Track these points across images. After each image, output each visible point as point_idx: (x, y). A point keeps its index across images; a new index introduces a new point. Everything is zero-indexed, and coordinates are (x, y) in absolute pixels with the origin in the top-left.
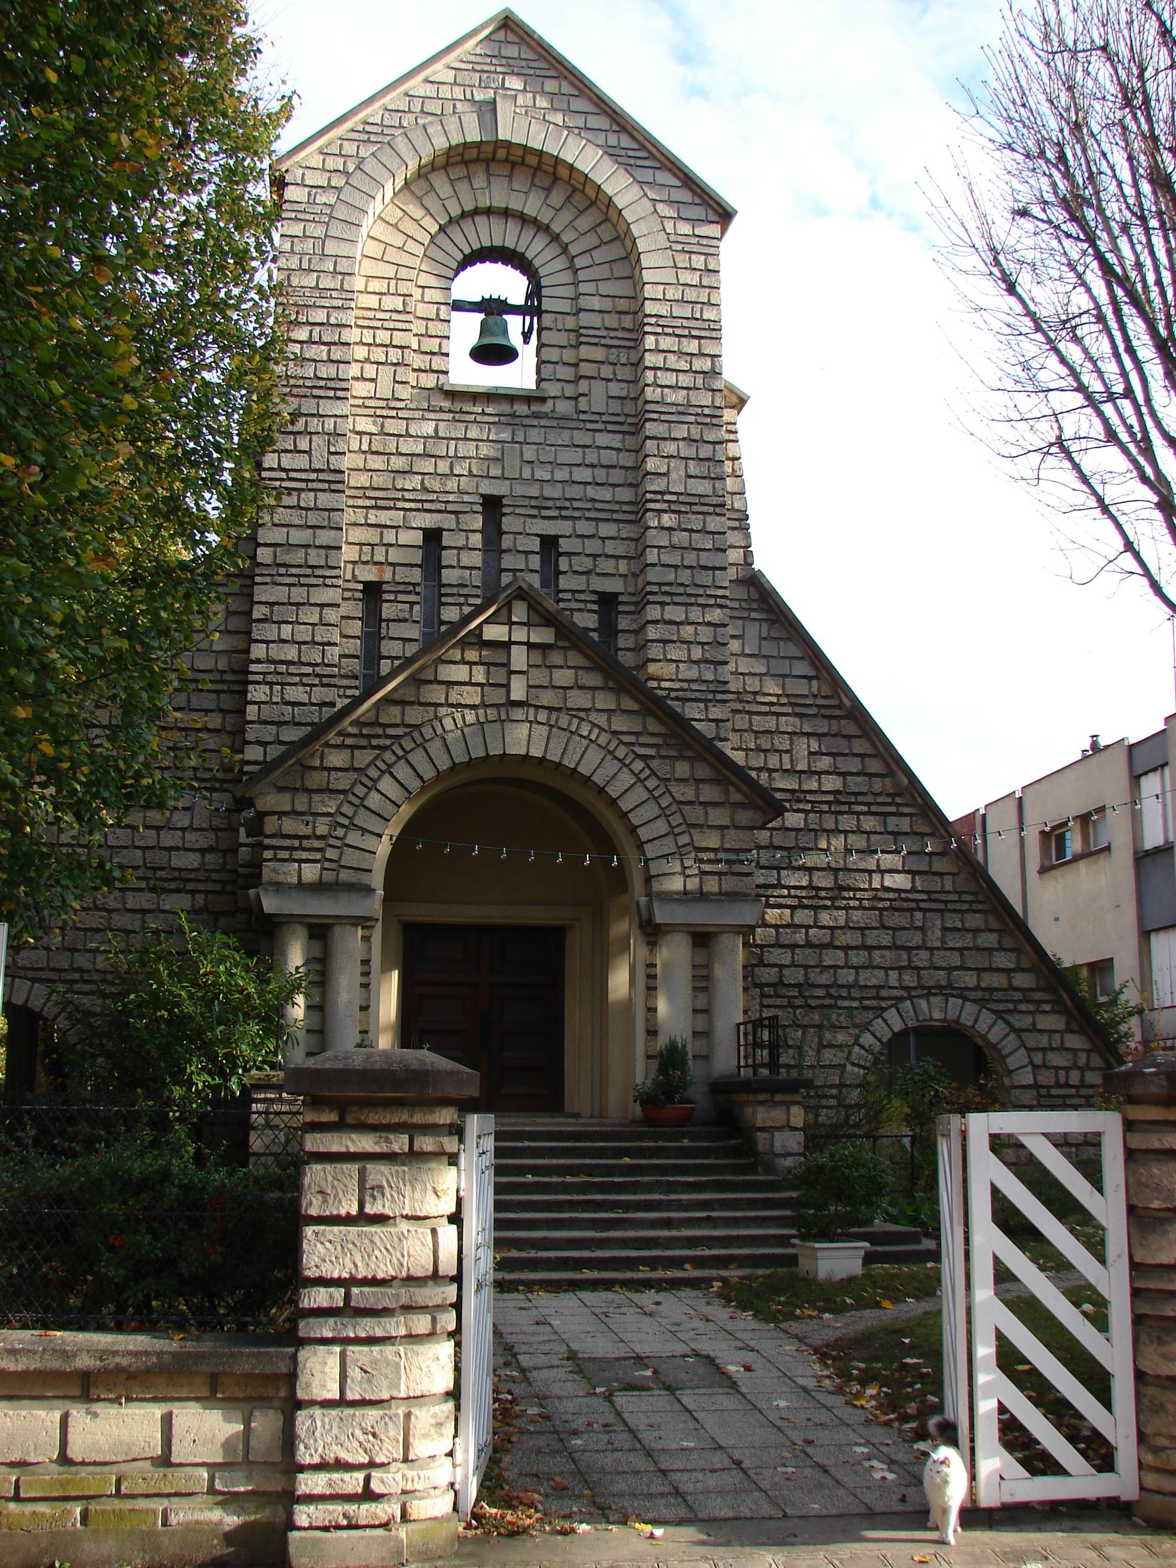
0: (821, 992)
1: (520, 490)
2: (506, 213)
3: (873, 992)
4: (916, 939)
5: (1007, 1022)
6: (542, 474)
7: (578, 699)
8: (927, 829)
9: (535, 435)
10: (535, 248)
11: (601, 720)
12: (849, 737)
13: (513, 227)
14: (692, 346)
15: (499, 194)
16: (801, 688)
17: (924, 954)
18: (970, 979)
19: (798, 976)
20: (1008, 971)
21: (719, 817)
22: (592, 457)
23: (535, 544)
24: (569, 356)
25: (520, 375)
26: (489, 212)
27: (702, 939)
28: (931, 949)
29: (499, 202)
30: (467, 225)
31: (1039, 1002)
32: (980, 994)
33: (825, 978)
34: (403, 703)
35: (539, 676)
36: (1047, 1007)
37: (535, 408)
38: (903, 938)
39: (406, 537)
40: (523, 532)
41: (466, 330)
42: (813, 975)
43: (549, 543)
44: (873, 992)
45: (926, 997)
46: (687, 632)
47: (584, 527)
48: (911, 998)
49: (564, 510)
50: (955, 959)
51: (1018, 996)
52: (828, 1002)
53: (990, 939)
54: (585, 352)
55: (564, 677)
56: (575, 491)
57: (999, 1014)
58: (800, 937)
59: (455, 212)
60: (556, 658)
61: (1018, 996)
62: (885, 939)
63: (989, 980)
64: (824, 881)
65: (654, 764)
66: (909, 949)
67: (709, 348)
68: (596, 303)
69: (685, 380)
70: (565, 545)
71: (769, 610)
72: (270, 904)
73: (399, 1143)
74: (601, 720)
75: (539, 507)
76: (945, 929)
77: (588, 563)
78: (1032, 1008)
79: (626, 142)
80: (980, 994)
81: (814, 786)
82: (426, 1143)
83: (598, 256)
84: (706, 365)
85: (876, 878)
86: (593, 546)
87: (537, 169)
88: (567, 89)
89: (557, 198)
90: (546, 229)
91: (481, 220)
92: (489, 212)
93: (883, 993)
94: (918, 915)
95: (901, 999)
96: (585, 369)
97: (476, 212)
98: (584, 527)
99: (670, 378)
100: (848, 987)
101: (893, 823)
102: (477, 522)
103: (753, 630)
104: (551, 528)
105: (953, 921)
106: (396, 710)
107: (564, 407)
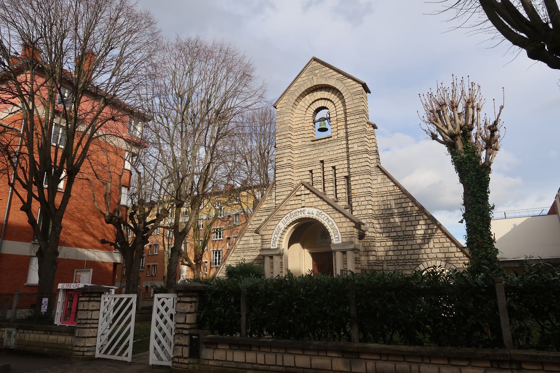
0: (402, 261)
1: (327, 158)
2: (322, 99)
3: (415, 261)
9: (329, 145)
11: (320, 207)
17: (429, 250)
19: (396, 258)
23: (331, 169)
26: (318, 100)
27: (344, 253)
33: (402, 258)
37: (330, 139)
39: (306, 173)
42: (400, 258)
44: (415, 261)
46: (360, 182)
47: (340, 163)
49: (336, 160)
52: (404, 263)
54: (339, 124)
55: (312, 200)
56: (338, 155)
59: (311, 102)
60: (311, 196)
64: (400, 234)
69: (356, 125)
70: (336, 168)
73: (88, 299)
74: (320, 207)
75: (331, 160)
79: (341, 75)
82: (92, 299)
88: (327, 68)
96: (339, 128)
97: (315, 101)
98: (340, 163)
99: (353, 125)
104: (333, 165)
107: (336, 137)
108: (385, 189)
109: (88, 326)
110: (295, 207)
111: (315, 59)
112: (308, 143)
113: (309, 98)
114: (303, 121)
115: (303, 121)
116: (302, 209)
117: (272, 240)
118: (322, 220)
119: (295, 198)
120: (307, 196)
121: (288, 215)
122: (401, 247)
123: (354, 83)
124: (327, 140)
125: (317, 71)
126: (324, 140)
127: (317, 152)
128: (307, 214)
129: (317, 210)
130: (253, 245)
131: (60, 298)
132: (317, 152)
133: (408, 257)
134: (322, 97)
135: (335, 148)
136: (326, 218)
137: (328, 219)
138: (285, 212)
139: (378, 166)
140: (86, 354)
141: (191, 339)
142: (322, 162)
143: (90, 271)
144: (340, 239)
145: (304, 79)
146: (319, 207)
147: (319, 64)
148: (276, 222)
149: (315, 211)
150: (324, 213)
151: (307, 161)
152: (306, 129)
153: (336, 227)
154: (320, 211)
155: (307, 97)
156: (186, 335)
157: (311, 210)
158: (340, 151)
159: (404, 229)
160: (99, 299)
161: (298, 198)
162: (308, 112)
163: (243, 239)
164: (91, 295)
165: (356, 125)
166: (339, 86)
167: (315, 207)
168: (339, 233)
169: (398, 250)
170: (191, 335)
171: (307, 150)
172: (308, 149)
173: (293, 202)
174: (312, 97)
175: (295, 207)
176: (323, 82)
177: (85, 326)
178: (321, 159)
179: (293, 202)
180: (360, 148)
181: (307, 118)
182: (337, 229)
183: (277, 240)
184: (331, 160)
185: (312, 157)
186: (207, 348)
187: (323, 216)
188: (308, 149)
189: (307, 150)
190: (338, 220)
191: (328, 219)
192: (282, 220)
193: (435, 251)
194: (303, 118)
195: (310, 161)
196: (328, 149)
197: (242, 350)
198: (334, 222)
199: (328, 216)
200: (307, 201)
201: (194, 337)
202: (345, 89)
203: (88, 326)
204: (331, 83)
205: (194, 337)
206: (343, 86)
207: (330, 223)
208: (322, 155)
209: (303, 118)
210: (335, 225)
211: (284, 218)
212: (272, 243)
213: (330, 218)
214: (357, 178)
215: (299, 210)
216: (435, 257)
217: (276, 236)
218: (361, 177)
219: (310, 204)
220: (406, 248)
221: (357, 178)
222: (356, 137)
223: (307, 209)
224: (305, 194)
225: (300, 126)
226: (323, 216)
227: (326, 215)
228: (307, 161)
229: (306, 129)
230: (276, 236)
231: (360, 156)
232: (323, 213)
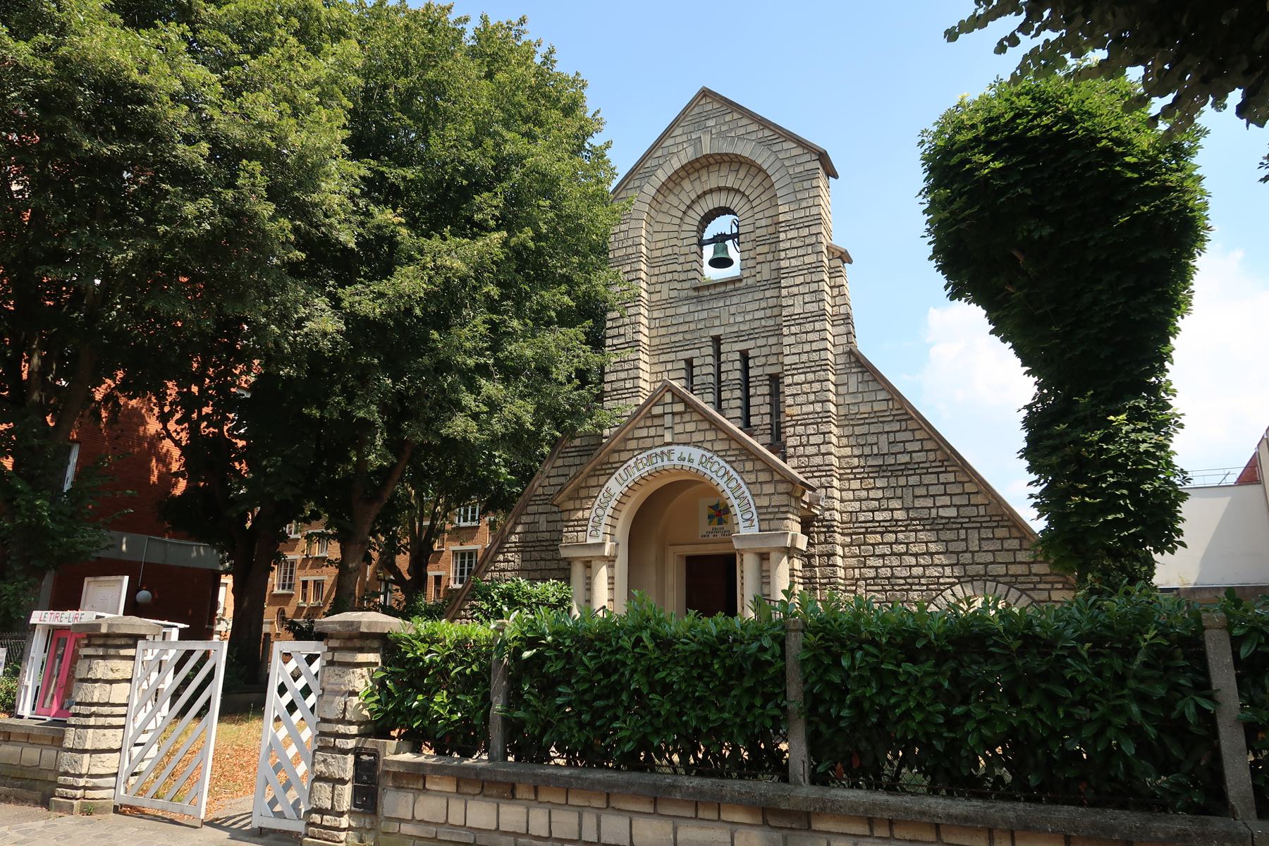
0: (902, 581)
1: (728, 330)
2: (720, 189)
4: (962, 546)
5: (1029, 596)
6: (740, 319)
7: (697, 437)
8: (967, 479)
9: (735, 300)
10: (735, 202)
11: (708, 446)
12: (913, 430)
13: (723, 195)
14: (805, 232)
15: (714, 180)
16: (883, 406)
18: (1001, 570)
19: (888, 572)
20: (1028, 563)
21: (768, 489)
22: (763, 304)
23: (737, 356)
24: (752, 254)
25: (733, 271)
28: (973, 553)
29: (714, 186)
30: (702, 202)
31: (1052, 583)
32: (1008, 579)
33: (905, 573)
34: (619, 451)
35: (678, 429)
36: (1060, 586)
37: (737, 285)
38: (952, 547)
39: (677, 365)
40: (731, 351)
41: (709, 252)
43: (745, 357)
45: (971, 582)
46: (806, 388)
47: (761, 342)
48: (960, 583)
49: (751, 335)
50: (990, 558)
51: (1036, 579)
53: (1014, 544)
56: (756, 324)
57: (1023, 591)
58: (887, 550)
59: (693, 196)
60: (687, 417)
61: (1036, 579)
62: (941, 547)
63: (1013, 569)
65: (735, 465)
66: (957, 553)
67: (814, 230)
68: (763, 223)
69: (801, 252)
70: (751, 353)
71: (862, 366)
72: (564, 553)
74: (708, 446)
75: (738, 336)
76: (980, 539)
77: (763, 360)
78: (1048, 586)
79: (767, 132)
80: (1008, 579)
81: (893, 462)
82: (112, 652)
83: (764, 197)
84: (813, 240)
85: (934, 511)
86: (765, 351)
87: (731, 162)
88: (736, 116)
89: (742, 174)
90: (737, 191)
91: (708, 197)
92: (711, 191)
93: (941, 580)
94: (963, 532)
95: (953, 584)
97: (705, 193)
98: (761, 342)
99: (793, 253)
100: (919, 578)
101: (943, 478)
102: (710, 351)
103: (853, 380)
105: (987, 533)
106: (616, 455)
107: (750, 281)
108: (865, 408)
109: (101, 721)
110: (648, 442)
111: (705, 93)
112: (684, 294)
113: (690, 189)
114: (674, 242)
115: (674, 242)
116: (665, 449)
117: (591, 523)
118: (714, 476)
119: (649, 423)
120: (677, 419)
121: (631, 462)
122: (902, 548)
123: (799, 151)
124: (731, 287)
125: (711, 123)
126: (722, 289)
127: (704, 315)
128: (676, 462)
129: (701, 452)
130: (547, 536)
131: (37, 648)
132: (704, 315)
133: (917, 571)
134: (722, 184)
135: (750, 307)
136: (722, 472)
137: (727, 473)
138: (624, 456)
139: (851, 353)
140: (90, 794)
141: (357, 763)
142: (717, 340)
143: (121, 581)
144: (756, 522)
145: (679, 140)
146: (705, 445)
147: (716, 105)
148: (602, 479)
149: (696, 453)
150: (719, 460)
151: (680, 337)
152: (682, 259)
153: (747, 494)
154: (709, 455)
155: (687, 185)
156: (345, 752)
157: (686, 451)
158: (760, 314)
159: (909, 504)
160: (131, 652)
161: (657, 422)
162: (687, 220)
163: (524, 519)
164: (110, 642)
165: (801, 252)
166: (763, 158)
167: (697, 445)
168: (753, 509)
169: (893, 554)
170: (357, 752)
171: (680, 311)
172: (685, 309)
173: (644, 433)
174: (697, 182)
175: (648, 442)
176: (726, 148)
177: (92, 721)
178: (714, 332)
179: (644, 433)
180: (809, 307)
181: (683, 235)
182: (750, 497)
183: (603, 522)
184: (738, 336)
185: (693, 326)
186: (399, 788)
187: (715, 467)
188: (685, 309)
189: (680, 311)
190: (752, 478)
191: (727, 473)
192: (616, 475)
193: (981, 558)
194: (675, 234)
195: (688, 336)
196: (733, 309)
197: (491, 796)
198: (740, 481)
199: (728, 467)
200: (678, 429)
201: (365, 758)
202: (778, 164)
203: (101, 721)
204: (744, 150)
205: (365, 758)
206: (772, 158)
207: (733, 484)
208: (717, 322)
209: (675, 234)
210: (744, 488)
211: (621, 471)
212: (590, 529)
213: (732, 472)
214: (798, 379)
215: (658, 450)
216: (982, 572)
217: (600, 512)
218: (810, 377)
219: (684, 438)
220: (914, 549)
221: (798, 379)
222: (800, 280)
223: (678, 450)
224: (673, 414)
225: (665, 252)
226: (715, 467)
227: (723, 463)
228: (680, 337)
229: (682, 259)
230: (600, 512)
231: (809, 327)
232: (715, 458)
